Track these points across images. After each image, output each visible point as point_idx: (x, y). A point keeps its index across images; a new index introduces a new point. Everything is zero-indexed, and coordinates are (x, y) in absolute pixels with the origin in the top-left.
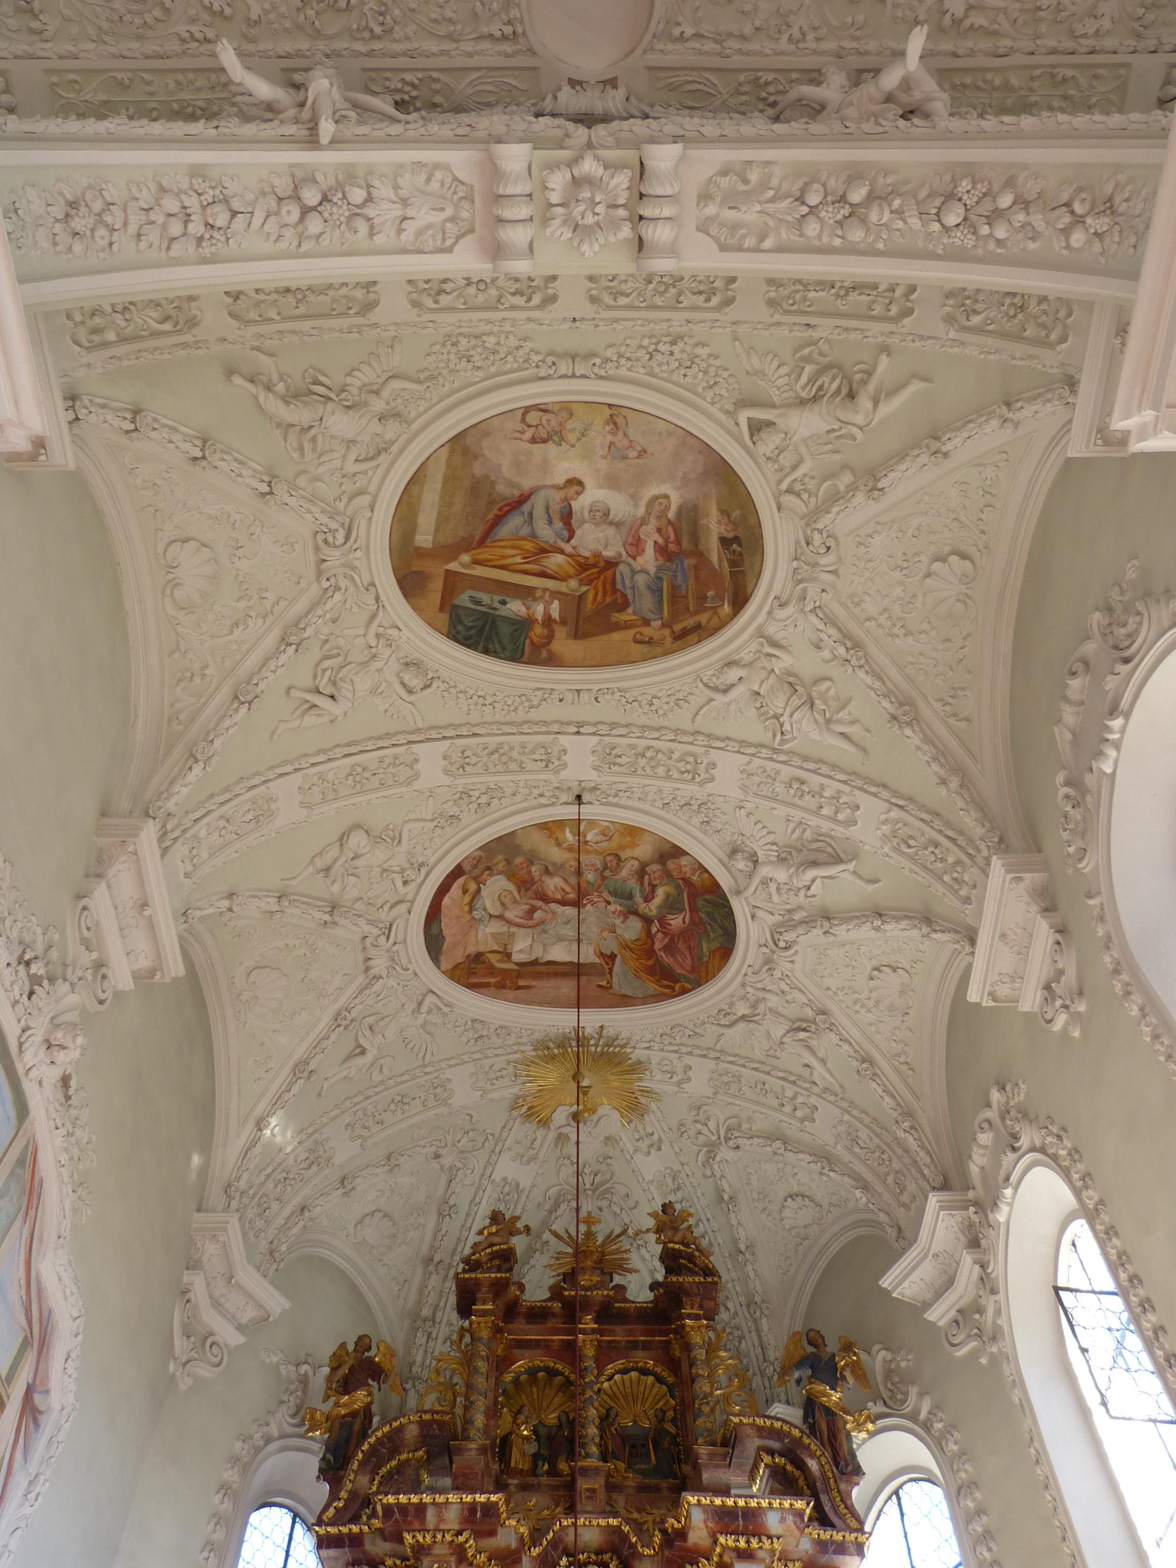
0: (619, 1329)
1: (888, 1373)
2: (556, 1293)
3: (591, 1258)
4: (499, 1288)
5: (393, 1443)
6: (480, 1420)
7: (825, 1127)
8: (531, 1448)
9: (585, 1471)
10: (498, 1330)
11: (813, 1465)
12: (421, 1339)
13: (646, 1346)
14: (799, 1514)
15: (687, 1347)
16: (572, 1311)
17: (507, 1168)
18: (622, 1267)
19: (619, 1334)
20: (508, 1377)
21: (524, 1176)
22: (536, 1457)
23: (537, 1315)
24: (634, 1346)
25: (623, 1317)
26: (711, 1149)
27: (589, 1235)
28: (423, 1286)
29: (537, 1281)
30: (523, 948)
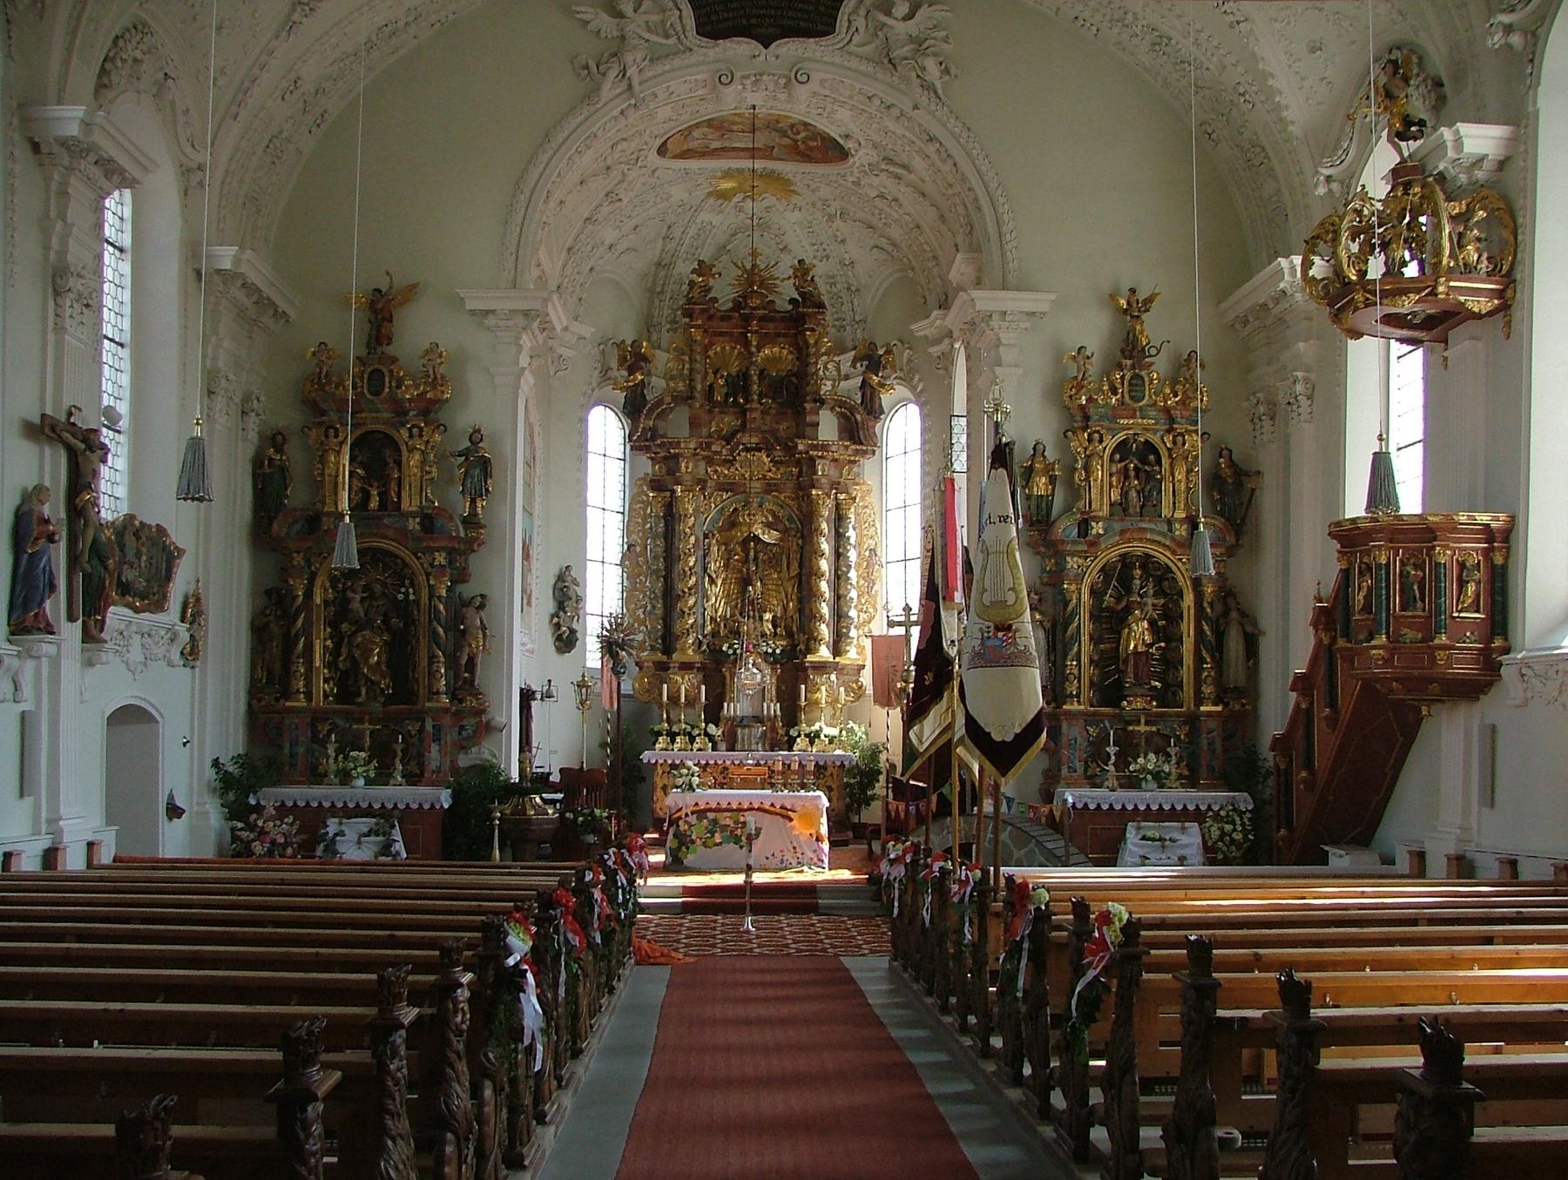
0: (771, 325)
1: (909, 361)
2: (738, 305)
3: (754, 279)
4: (703, 311)
5: (659, 402)
6: (699, 387)
7: (895, 233)
8: (724, 390)
9: (751, 410)
10: (705, 331)
11: (858, 417)
12: (656, 303)
13: (785, 335)
14: (847, 447)
15: (806, 342)
16: (747, 319)
17: (704, 216)
18: (771, 289)
19: (771, 328)
20: (711, 353)
21: (716, 220)
22: (727, 395)
23: (726, 318)
24: (778, 335)
25: (772, 320)
26: (831, 218)
27: (754, 266)
28: (656, 276)
29: (724, 292)
30: (715, 145)
